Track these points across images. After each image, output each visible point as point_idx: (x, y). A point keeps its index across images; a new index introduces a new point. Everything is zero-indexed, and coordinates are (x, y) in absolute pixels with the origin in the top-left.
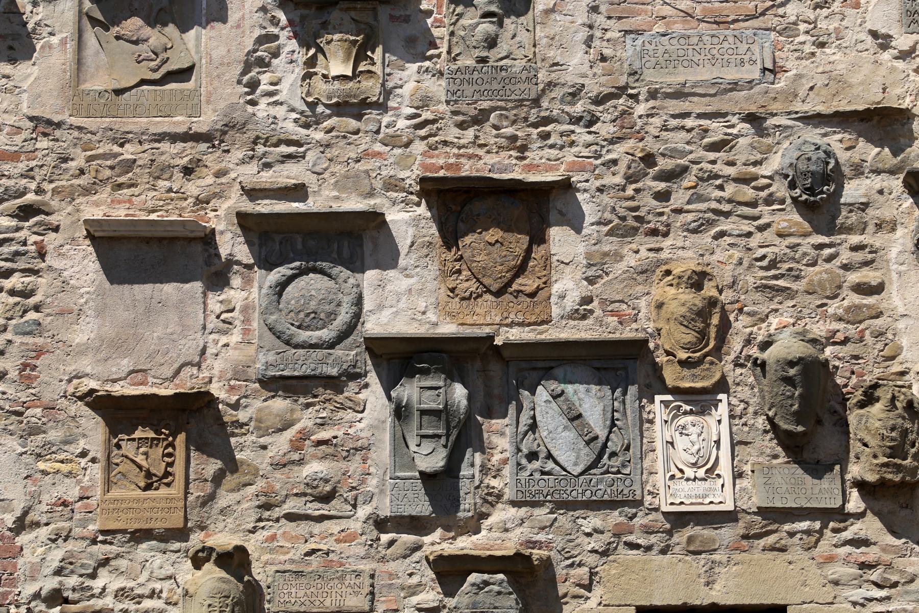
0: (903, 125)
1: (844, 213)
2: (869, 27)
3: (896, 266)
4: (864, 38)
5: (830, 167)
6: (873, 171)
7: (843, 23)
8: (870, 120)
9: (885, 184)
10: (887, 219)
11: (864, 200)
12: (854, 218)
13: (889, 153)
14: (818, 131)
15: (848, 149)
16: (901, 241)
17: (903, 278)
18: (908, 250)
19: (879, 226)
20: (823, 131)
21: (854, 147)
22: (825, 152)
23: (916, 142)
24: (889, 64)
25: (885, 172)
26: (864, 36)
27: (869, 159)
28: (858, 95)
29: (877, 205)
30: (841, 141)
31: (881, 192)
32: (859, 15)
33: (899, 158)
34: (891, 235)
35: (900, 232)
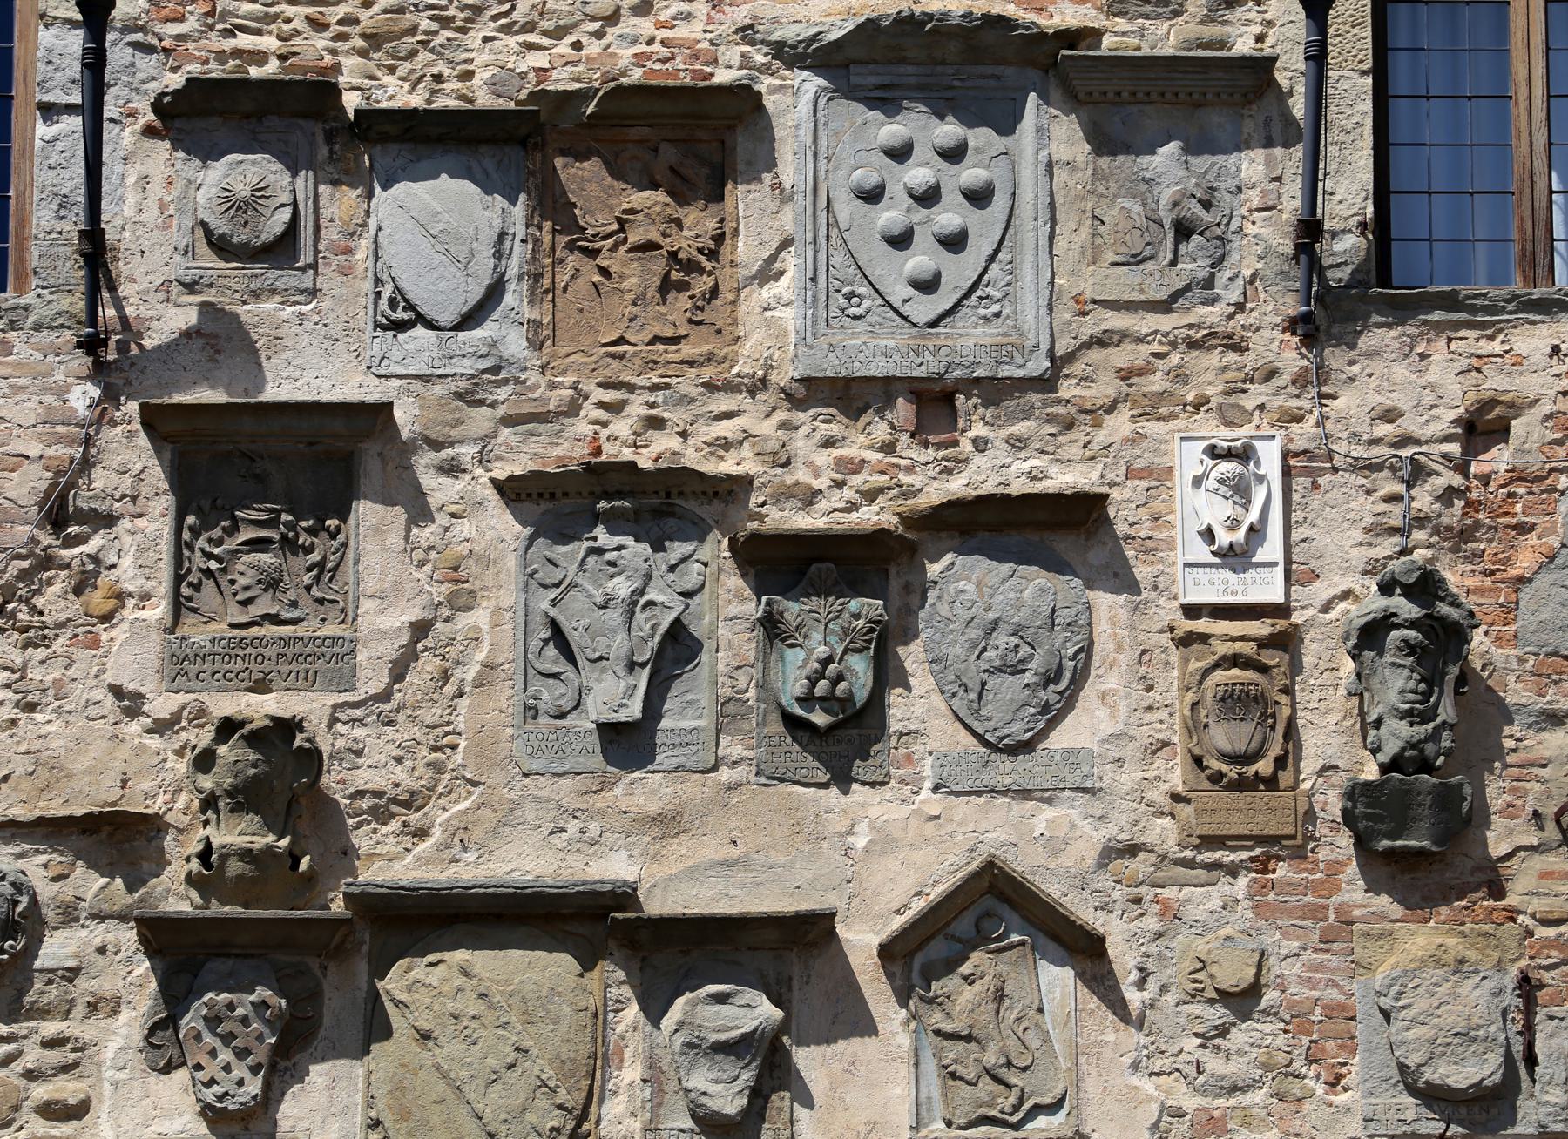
0: (150, 840)
1: (38, 985)
2: (110, 680)
3: (110, 1073)
4: (101, 697)
5: (19, 909)
6: (93, 916)
7: (68, 673)
8: (96, 831)
9: (110, 937)
10: (107, 995)
11: (72, 964)
12: (53, 992)
13: (122, 886)
14: (10, 849)
15: (55, 879)
16: (123, 1031)
17: (120, 1092)
18: (133, 1045)
19: (93, 1007)
20: (17, 849)
21: (67, 876)
22: (13, 884)
23: (168, 868)
24: (136, 741)
25: (112, 917)
26: (100, 694)
27: (89, 896)
28: (81, 792)
29: (93, 972)
30: (45, 866)
31: (102, 950)
32: (96, 660)
33: (136, 895)
34: (110, 1020)
35: (125, 1015)
